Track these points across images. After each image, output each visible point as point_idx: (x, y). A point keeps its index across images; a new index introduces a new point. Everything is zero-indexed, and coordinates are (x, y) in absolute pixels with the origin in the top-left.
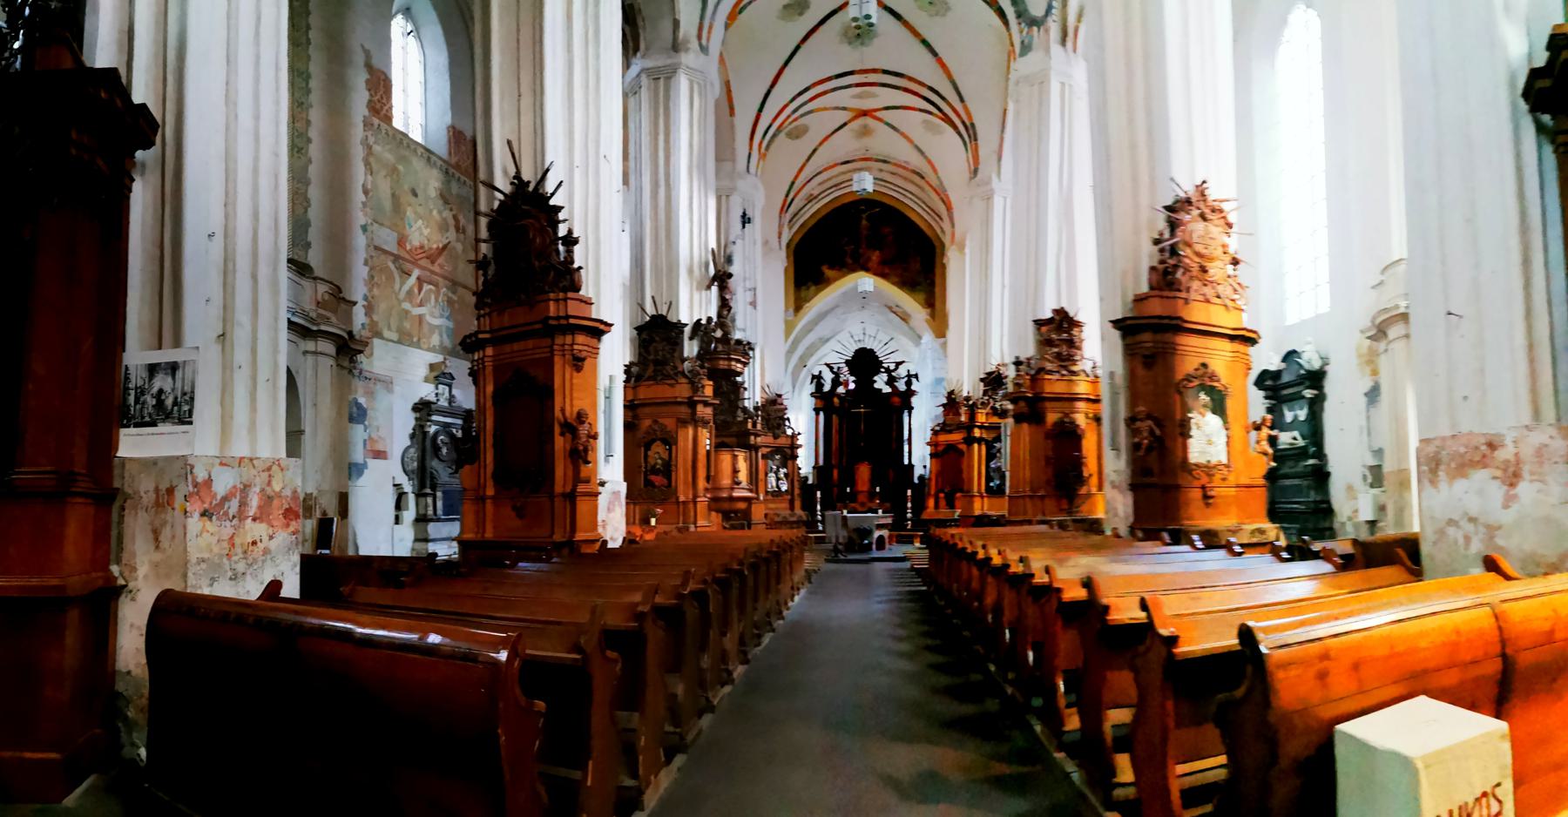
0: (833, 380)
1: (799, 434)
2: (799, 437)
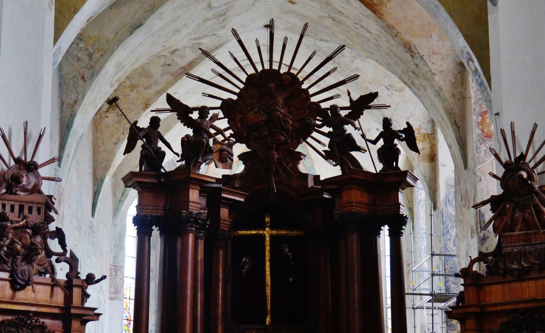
0: (186, 142)
1: (91, 279)
2: (90, 290)
